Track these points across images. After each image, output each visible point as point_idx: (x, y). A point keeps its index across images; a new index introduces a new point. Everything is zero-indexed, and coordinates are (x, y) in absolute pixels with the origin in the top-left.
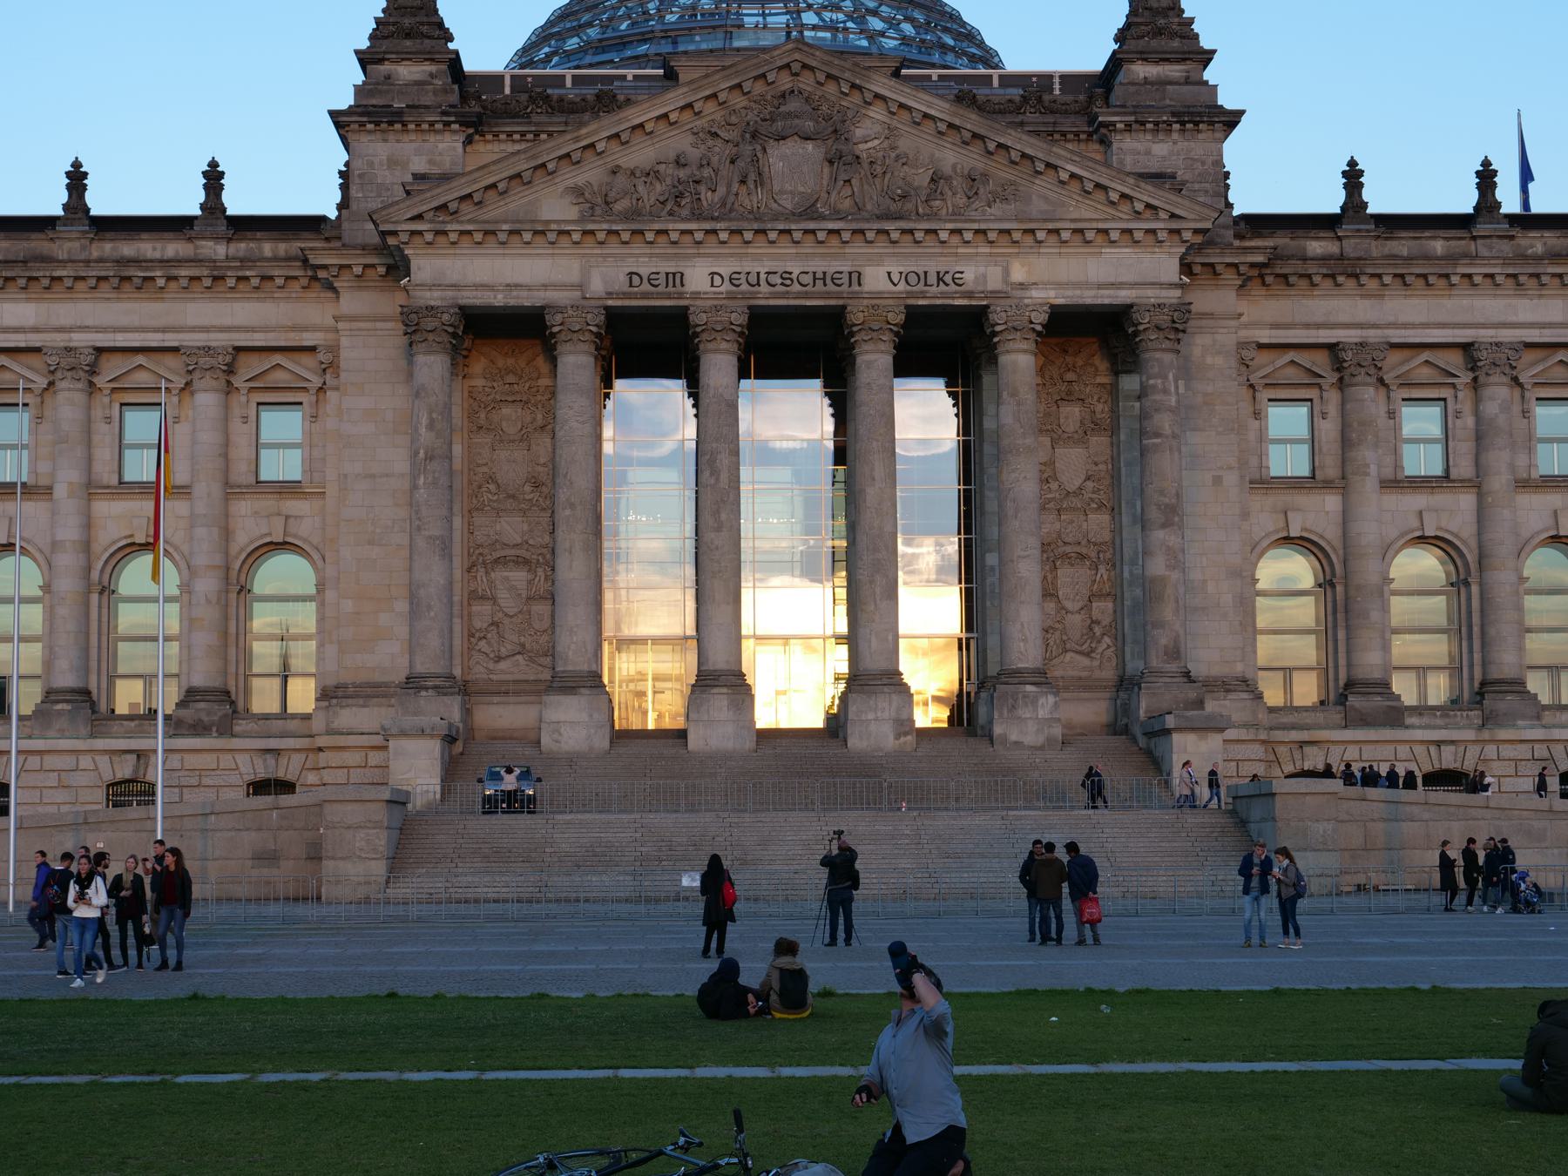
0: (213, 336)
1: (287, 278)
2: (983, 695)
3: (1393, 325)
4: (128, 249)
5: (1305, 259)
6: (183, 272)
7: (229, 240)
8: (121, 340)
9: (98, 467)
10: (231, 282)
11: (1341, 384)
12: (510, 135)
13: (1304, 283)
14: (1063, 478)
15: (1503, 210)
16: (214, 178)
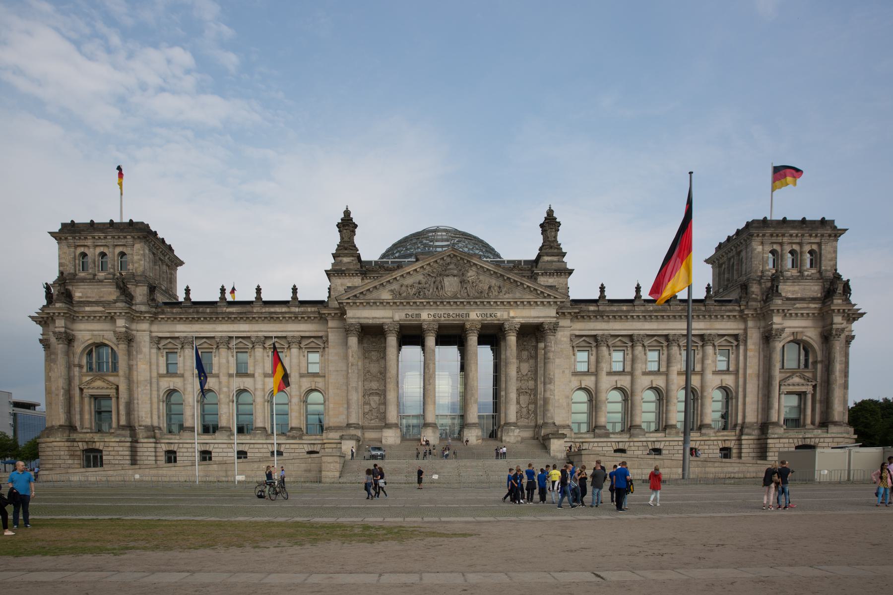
0: (295, 333)
1: (315, 317)
2: (500, 430)
3: (613, 330)
4: (272, 310)
5: (589, 311)
6: (287, 316)
7: (299, 307)
8: (270, 334)
9: (266, 369)
10: (300, 318)
11: (597, 346)
12: (374, 277)
13: (588, 318)
14: (522, 371)
15: (643, 298)
16: (295, 290)
